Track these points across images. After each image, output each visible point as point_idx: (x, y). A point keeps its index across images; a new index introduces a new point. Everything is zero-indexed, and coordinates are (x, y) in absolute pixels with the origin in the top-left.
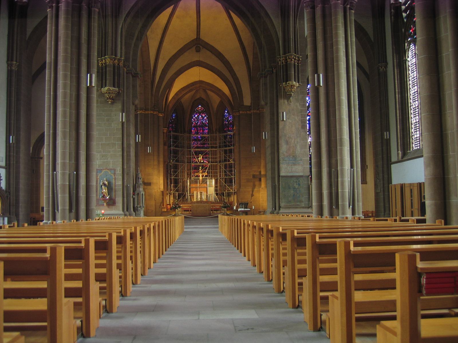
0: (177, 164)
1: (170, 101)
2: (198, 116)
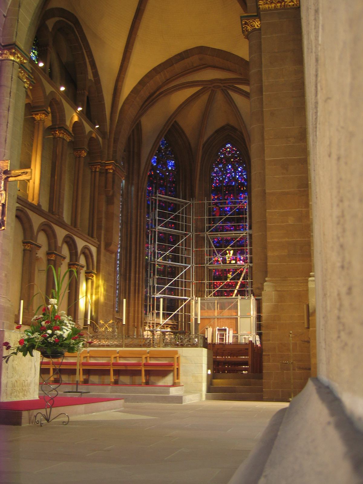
0: (175, 267)
1: (127, 99)
2: (224, 167)
